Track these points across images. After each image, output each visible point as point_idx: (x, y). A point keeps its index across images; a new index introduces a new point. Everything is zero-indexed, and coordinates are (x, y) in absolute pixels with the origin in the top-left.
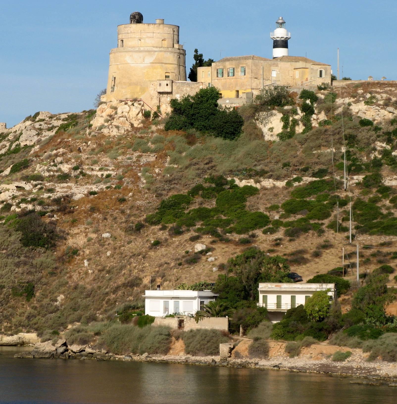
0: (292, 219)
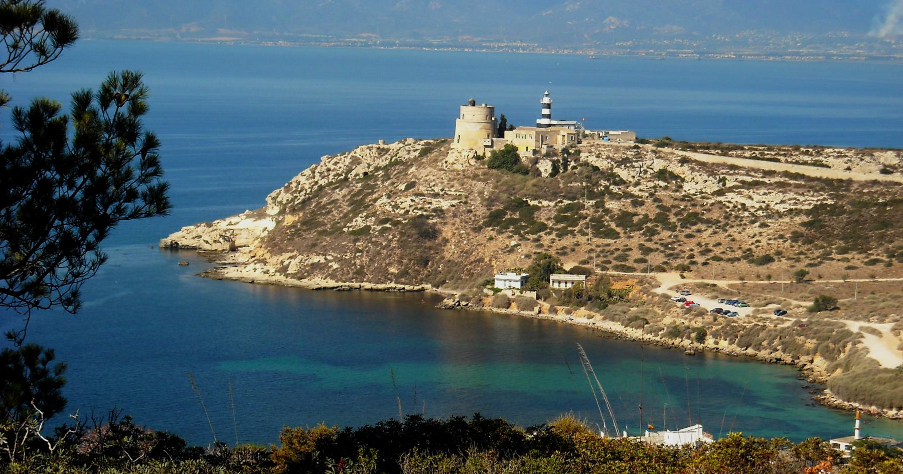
0: (559, 227)
